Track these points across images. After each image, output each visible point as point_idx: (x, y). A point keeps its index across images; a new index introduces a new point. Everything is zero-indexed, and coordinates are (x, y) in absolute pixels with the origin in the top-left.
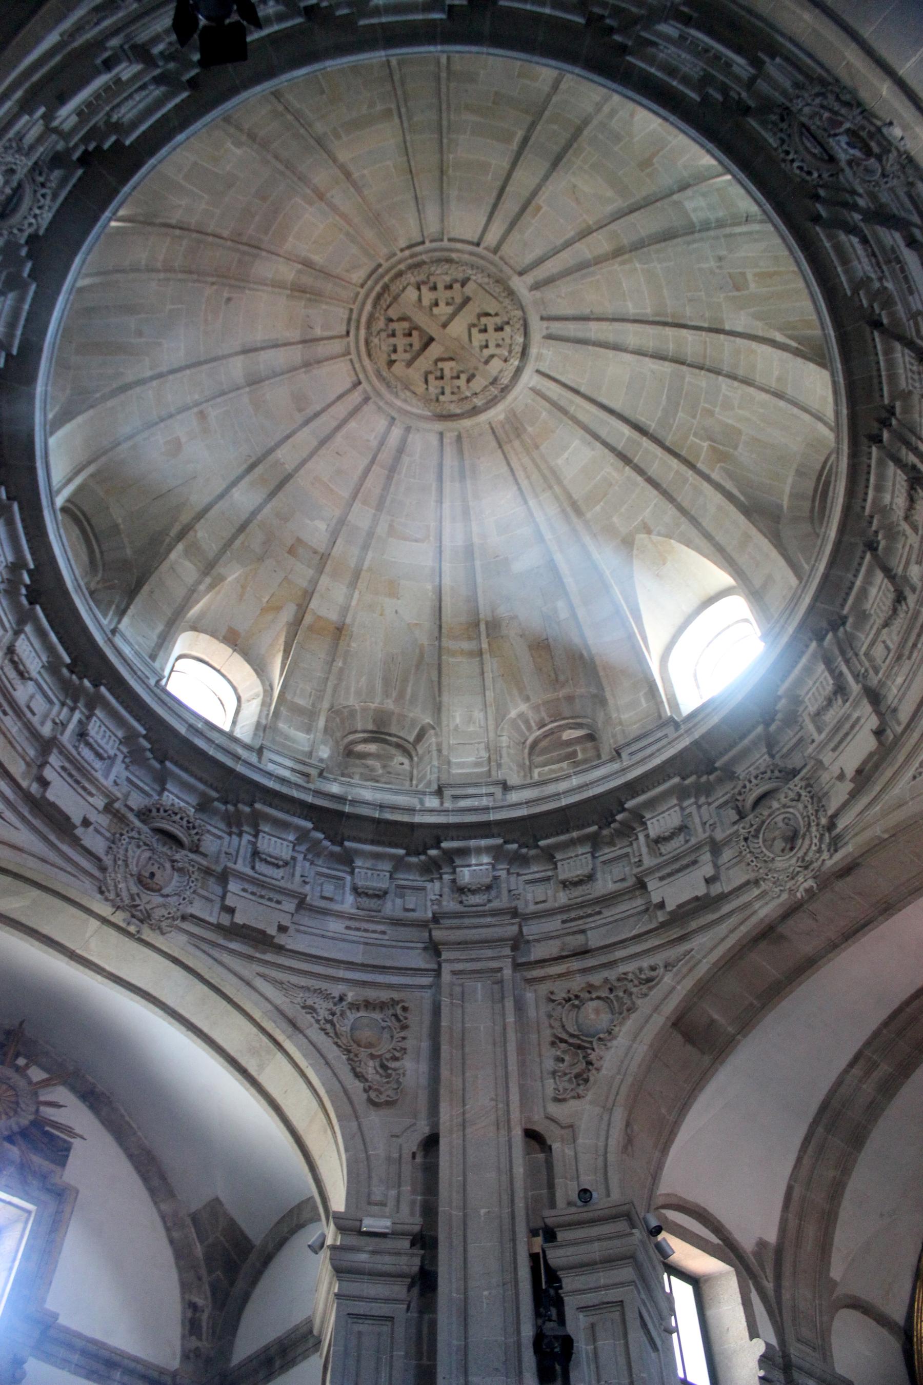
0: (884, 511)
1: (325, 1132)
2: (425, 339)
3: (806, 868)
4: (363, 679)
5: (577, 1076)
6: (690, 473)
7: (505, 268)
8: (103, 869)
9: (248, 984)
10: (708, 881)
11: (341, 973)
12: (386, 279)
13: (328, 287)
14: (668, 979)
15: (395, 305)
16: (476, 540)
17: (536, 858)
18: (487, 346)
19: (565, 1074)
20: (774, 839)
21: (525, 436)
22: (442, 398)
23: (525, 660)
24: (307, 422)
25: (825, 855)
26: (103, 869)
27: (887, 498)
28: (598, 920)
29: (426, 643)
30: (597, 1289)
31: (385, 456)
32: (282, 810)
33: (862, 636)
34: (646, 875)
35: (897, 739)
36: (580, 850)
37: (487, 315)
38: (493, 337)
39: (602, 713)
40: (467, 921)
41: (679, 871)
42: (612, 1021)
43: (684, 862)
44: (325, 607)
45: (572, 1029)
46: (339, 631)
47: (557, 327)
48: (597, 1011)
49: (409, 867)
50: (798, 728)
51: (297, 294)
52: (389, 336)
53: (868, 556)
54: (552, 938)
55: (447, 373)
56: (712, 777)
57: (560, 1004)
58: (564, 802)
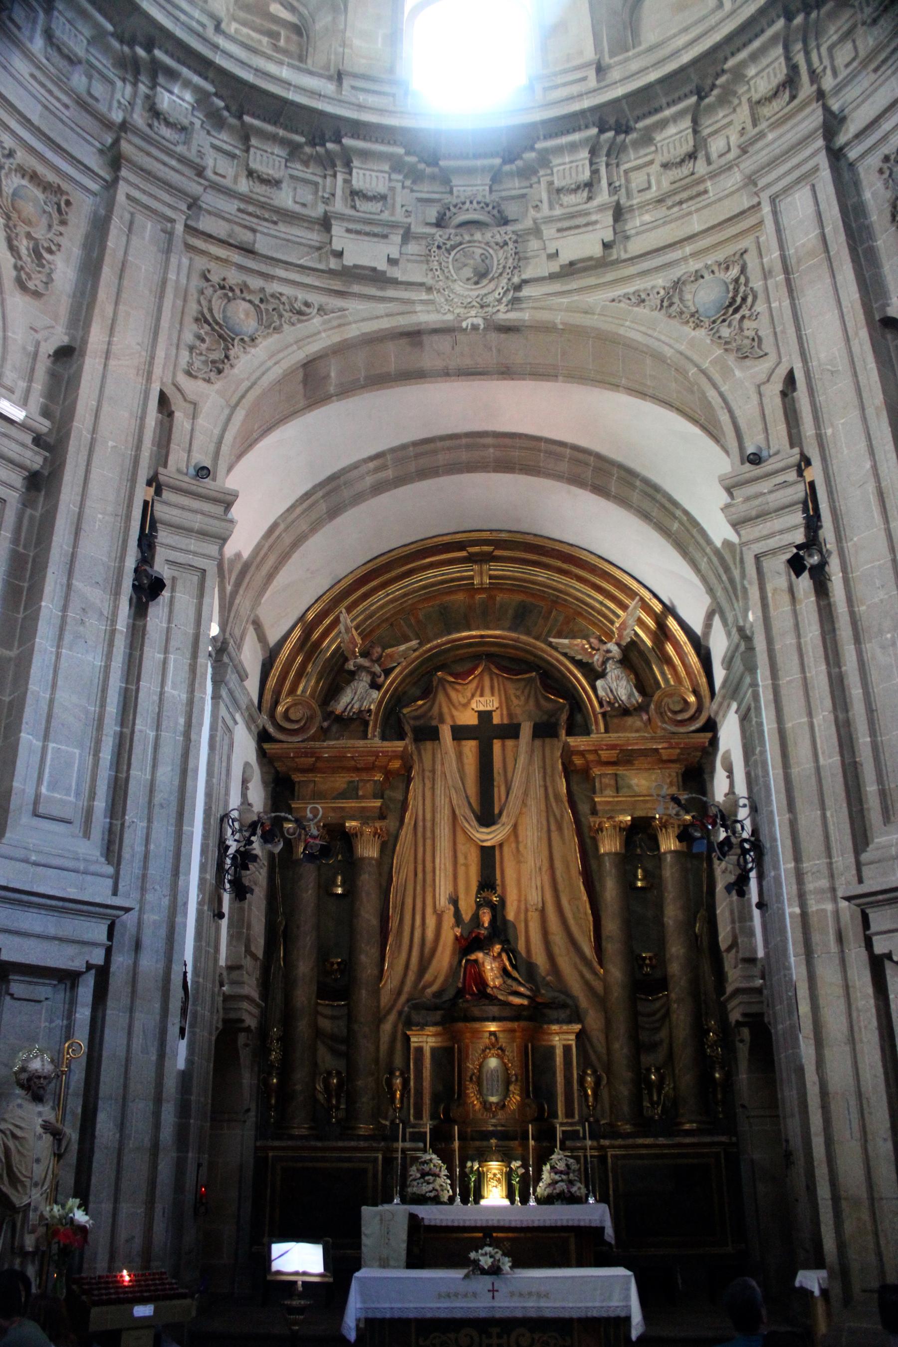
3: (482, 307)
11: (13, 124)
14: (317, 321)
17: (231, 128)
19: (201, 354)
20: (465, 265)
25: (502, 308)
27: (751, 71)
28: (272, 229)
30: (188, 552)
33: (632, 156)
34: (336, 218)
35: (618, 262)
36: (277, 150)
39: (329, 18)
41: (367, 234)
42: (257, 330)
43: (376, 230)
45: (219, 317)
48: (247, 315)
49: (107, 50)
50: (527, 184)
53: (694, 99)
54: (224, 218)
56: (429, 170)
57: (213, 286)
58: (291, 96)
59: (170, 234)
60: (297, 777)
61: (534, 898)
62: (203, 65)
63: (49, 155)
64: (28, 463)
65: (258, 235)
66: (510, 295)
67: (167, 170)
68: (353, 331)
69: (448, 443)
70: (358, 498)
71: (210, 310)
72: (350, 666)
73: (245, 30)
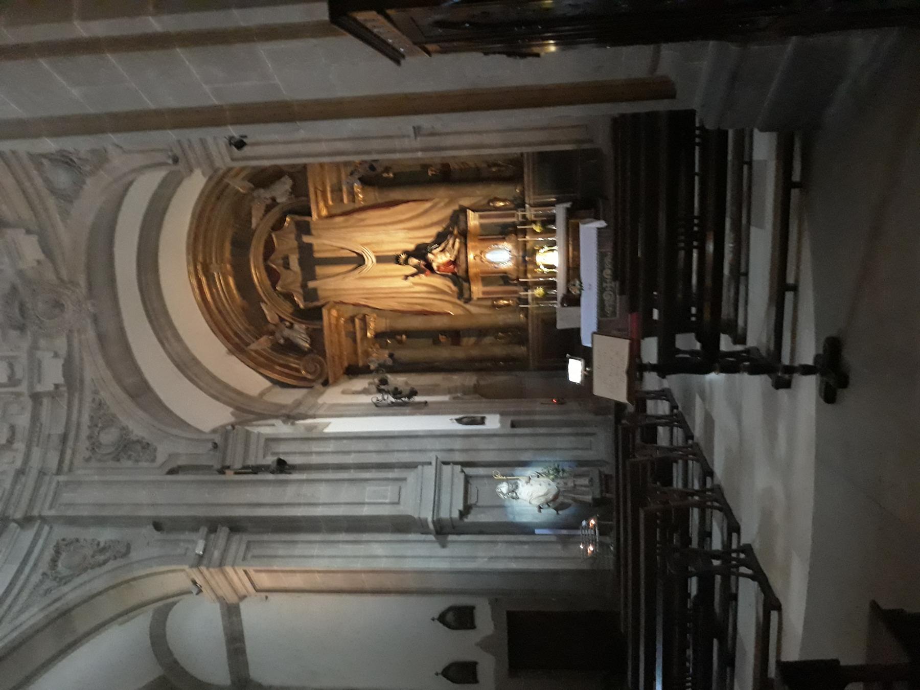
5: (143, 448)
10: (56, 355)
11: (23, 577)
14: (103, 394)
45: (112, 449)
59: (67, 483)
60: (346, 364)
61: (401, 235)
66: (69, 285)
68: (107, 374)
71: (109, 454)
72: (282, 341)
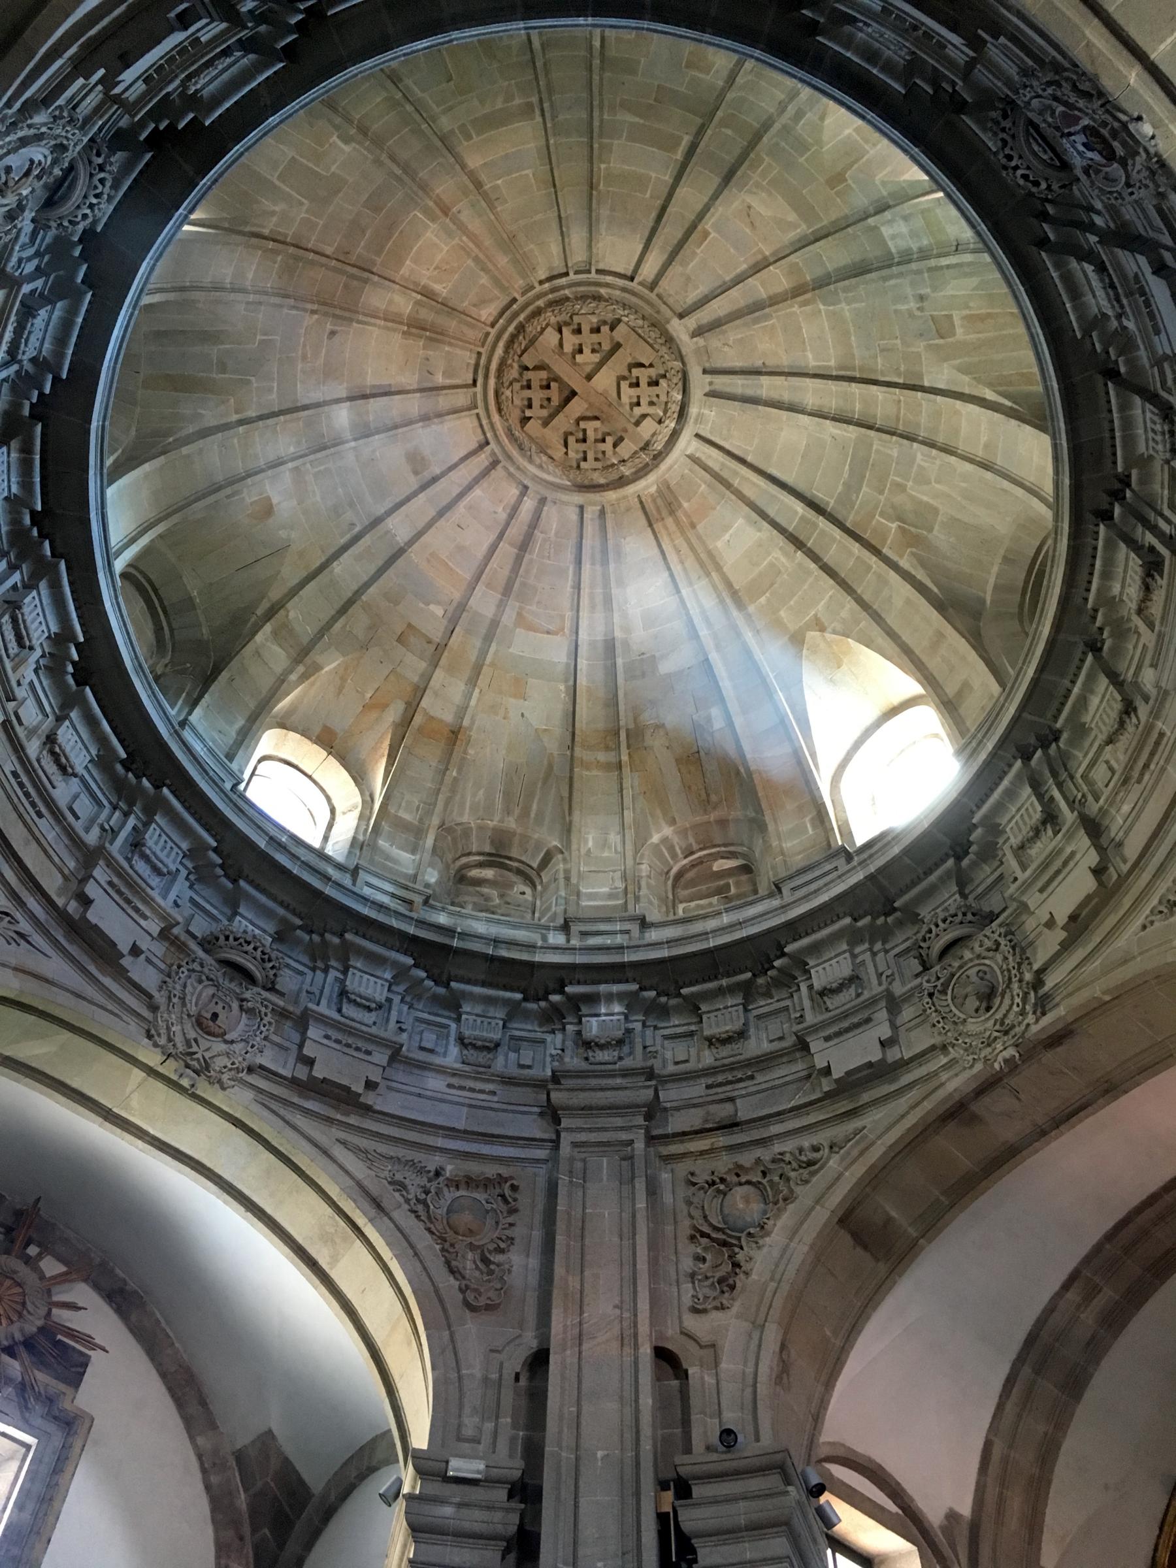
0: (1112, 603)
1: (409, 1344)
2: (566, 393)
3: (1006, 1033)
4: (481, 792)
5: (721, 1281)
6: (873, 560)
7: (663, 308)
8: (154, 1008)
9: (326, 1153)
11: (440, 1142)
12: (522, 317)
13: (452, 325)
14: (834, 1163)
15: (531, 350)
16: (618, 634)
17: (678, 1010)
18: (638, 404)
19: (707, 1278)
20: (966, 996)
21: (680, 514)
22: (583, 464)
23: (673, 779)
24: (423, 487)
25: (1031, 1018)
26: (154, 1008)
27: (1116, 589)
29: (556, 753)
31: (516, 531)
32: (377, 942)
33: (1080, 755)
34: (809, 1034)
35: (1123, 879)
37: (642, 365)
38: (645, 391)
40: (593, 1082)
41: (848, 1030)
42: (765, 1212)
43: (855, 1020)
44: (439, 705)
45: (716, 1221)
46: (455, 735)
47: (721, 383)
48: (747, 1201)
49: (527, 1015)
50: (997, 863)
51: (414, 330)
52: (522, 388)
53: (1090, 657)
54: (695, 1106)
55: (591, 435)
56: (890, 919)
57: (702, 1188)
62: (616, 972)
63: (486, 1149)
64: (500, 1528)
65: (738, 1101)
67: (608, 1094)
69: (1149, 1214)
70: (1095, 1349)
73: (693, 904)
